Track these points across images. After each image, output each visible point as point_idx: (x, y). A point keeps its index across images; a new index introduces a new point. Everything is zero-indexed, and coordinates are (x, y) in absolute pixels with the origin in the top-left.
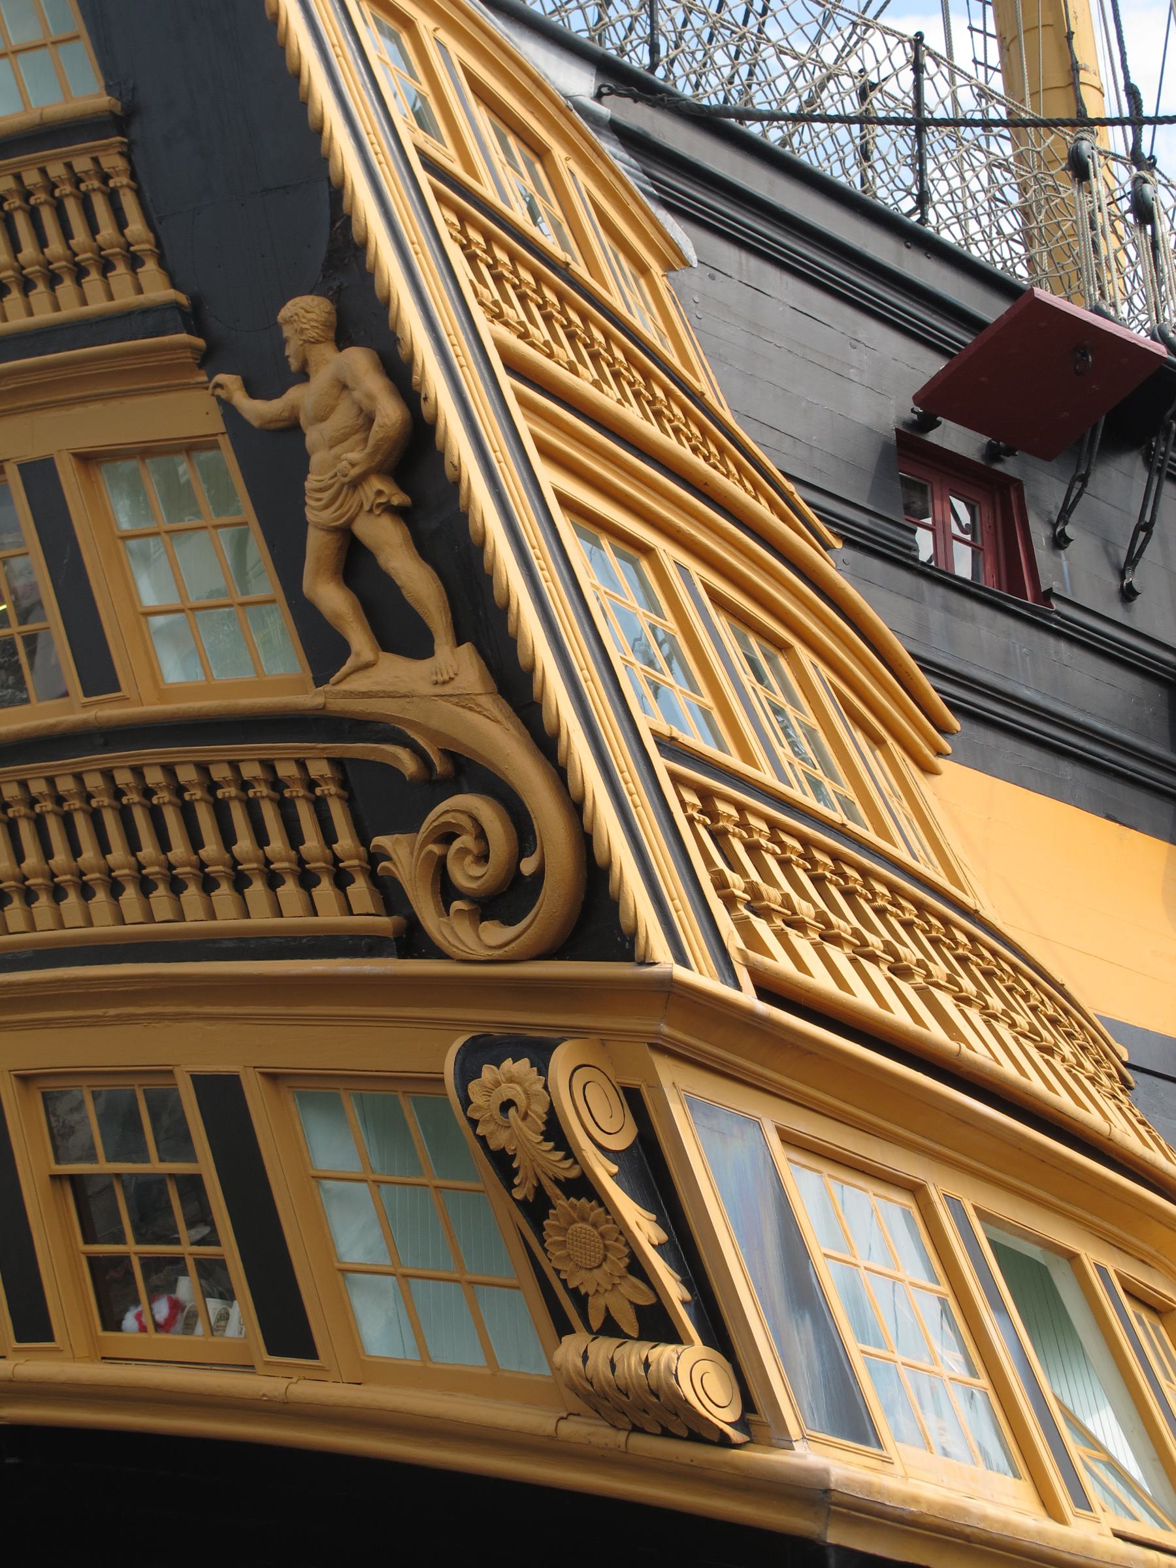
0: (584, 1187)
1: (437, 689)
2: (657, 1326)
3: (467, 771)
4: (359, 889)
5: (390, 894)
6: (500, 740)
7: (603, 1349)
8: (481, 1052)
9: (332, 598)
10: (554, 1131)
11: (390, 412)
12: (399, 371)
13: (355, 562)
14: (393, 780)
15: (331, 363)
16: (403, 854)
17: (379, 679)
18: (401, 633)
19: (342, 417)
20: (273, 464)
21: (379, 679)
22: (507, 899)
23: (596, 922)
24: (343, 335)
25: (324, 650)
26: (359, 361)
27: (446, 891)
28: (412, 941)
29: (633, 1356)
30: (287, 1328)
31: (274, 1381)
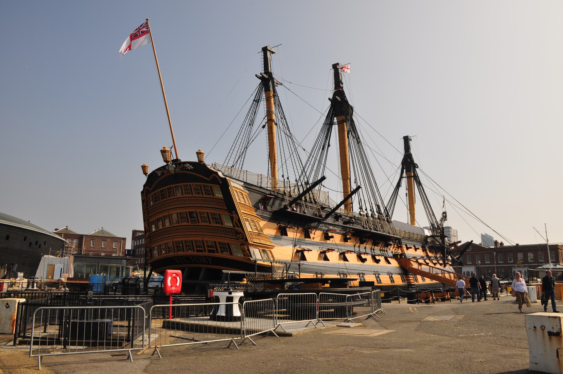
8: (241, 245)
13: (236, 223)
14: (237, 233)
17: (237, 228)
18: (238, 227)
21: (237, 228)
22: (243, 239)
23: (247, 240)
30: (231, 254)
31: (230, 256)
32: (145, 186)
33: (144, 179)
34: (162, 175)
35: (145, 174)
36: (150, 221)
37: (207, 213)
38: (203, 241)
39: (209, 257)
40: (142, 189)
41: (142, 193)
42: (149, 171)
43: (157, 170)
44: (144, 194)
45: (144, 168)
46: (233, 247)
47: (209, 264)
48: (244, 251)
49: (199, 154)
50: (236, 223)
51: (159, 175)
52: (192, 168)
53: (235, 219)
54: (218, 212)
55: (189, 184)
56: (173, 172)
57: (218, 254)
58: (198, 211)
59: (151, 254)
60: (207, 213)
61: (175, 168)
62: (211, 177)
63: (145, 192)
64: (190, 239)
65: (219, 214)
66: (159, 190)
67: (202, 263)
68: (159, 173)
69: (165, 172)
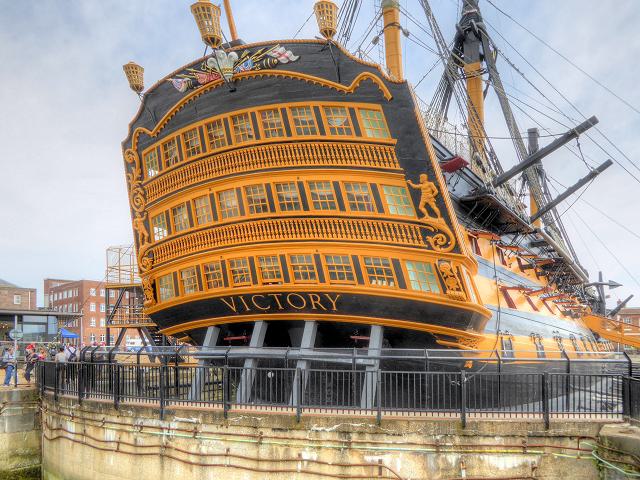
0: (454, 276)
1: (439, 222)
2: (458, 290)
3: (440, 231)
4: (422, 241)
5: (428, 243)
6: (446, 228)
7: (452, 292)
9: (424, 210)
10: (451, 270)
11: (437, 191)
12: (438, 188)
13: (427, 206)
15: (427, 184)
16: (431, 240)
18: (435, 216)
19: (429, 190)
20: (416, 195)
22: (446, 245)
24: (429, 180)
25: (420, 215)
26: (432, 183)
27: (436, 243)
28: (430, 248)
29: (457, 293)
30: (403, 285)
32: (132, 126)
33: (133, 104)
34: (190, 88)
35: (137, 88)
36: (152, 214)
37: (336, 184)
38: (317, 257)
39: (333, 295)
40: (125, 136)
41: (126, 145)
42: (148, 84)
43: (173, 76)
44: (138, 145)
45: (132, 70)
46: (411, 273)
47: (329, 310)
48: (442, 279)
49: (323, 9)
50: (427, 206)
51: (182, 88)
52: (294, 58)
53: (427, 196)
54: (370, 180)
55: (279, 106)
56: (229, 76)
57: (323, 285)
58: (304, 179)
59: (155, 292)
60: (336, 184)
61: (236, 64)
62: (355, 82)
63: (134, 141)
64: (278, 252)
65: (374, 187)
66: (179, 133)
67: (309, 308)
68: (181, 85)
69: (202, 77)
